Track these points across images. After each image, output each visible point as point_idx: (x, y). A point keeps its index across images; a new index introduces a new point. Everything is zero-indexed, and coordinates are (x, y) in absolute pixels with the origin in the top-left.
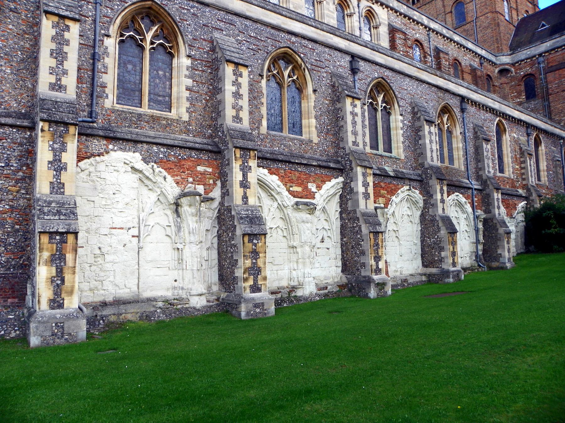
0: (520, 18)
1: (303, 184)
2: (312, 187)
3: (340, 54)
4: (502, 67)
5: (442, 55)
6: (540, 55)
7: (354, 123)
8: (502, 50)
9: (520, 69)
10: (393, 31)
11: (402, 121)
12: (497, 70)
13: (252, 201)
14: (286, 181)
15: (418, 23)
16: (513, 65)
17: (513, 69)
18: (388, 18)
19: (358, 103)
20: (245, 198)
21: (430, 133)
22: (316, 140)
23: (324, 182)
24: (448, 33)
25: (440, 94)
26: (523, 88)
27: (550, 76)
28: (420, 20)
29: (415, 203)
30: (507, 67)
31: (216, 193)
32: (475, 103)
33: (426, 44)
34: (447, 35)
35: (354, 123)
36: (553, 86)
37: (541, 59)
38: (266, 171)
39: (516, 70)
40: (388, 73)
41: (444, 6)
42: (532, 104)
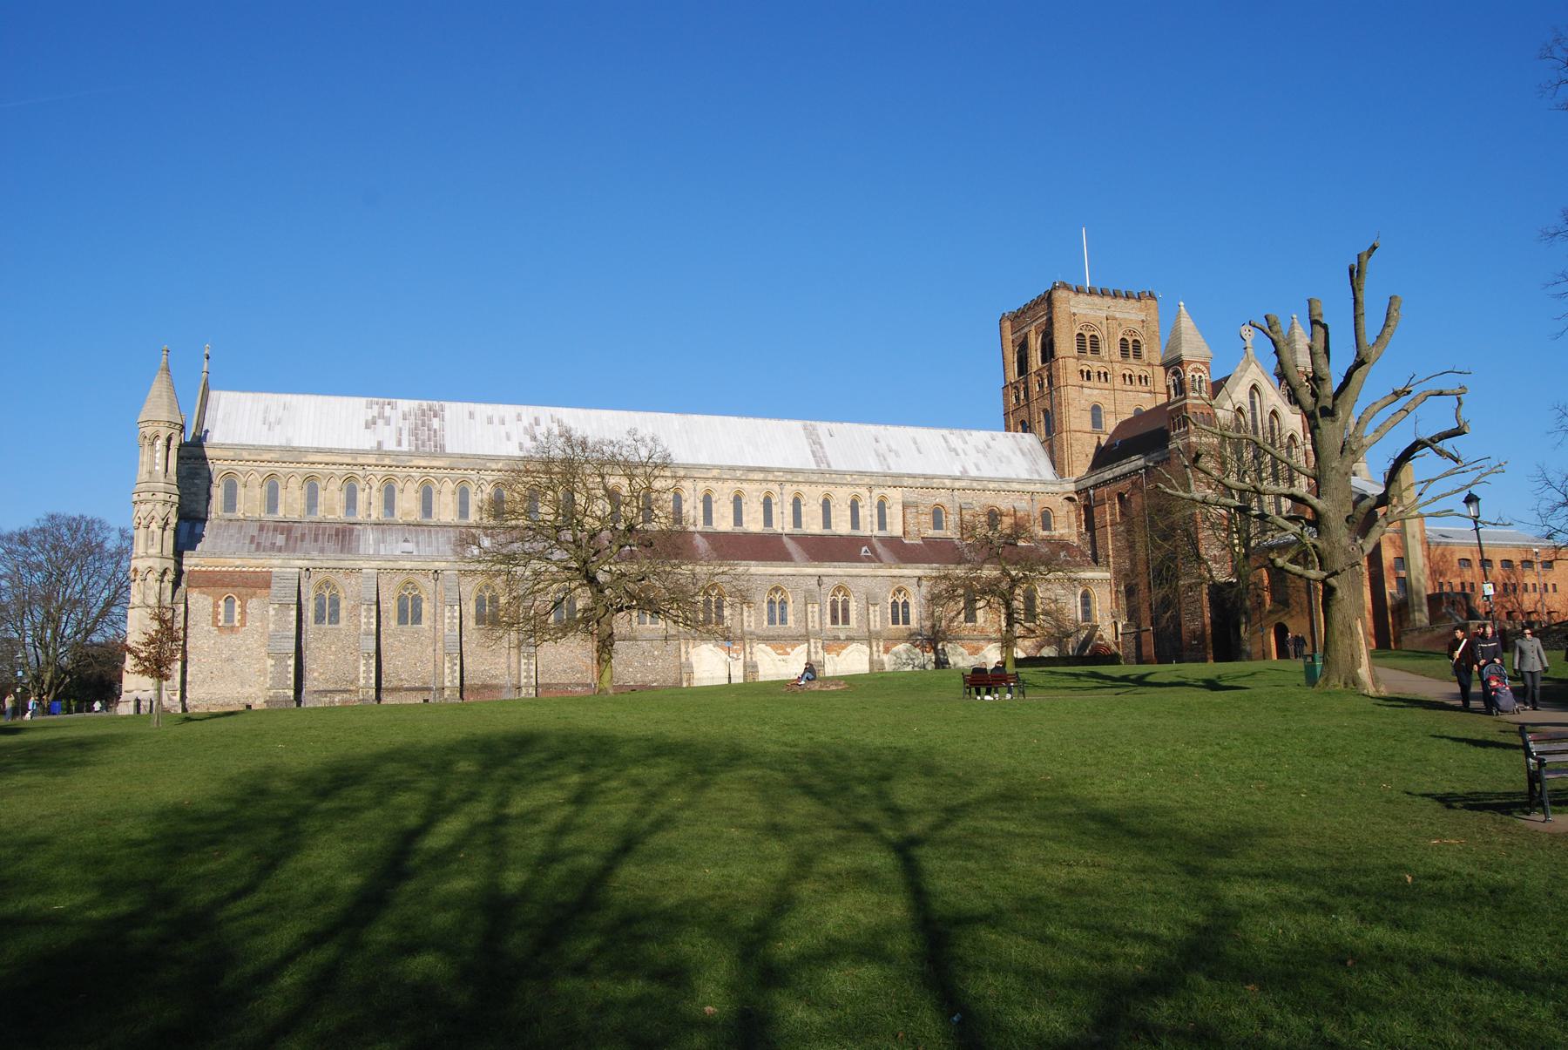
0: (1118, 422)
1: (782, 648)
2: (789, 650)
3: (810, 578)
5: (964, 512)
7: (813, 617)
10: (905, 506)
11: (857, 606)
12: (1061, 499)
13: (754, 659)
14: (775, 648)
15: (938, 489)
16: (1077, 492)
17: (1076, 498)
18: (903, 497)
19: (816, 606)
20: (751, 658)
21: (874, 611)
22: (793, 626)
23: (795, 647)
24: (979, 485)
25: (894, 580)
28: (941, 486)
29: (864, 652)
31: (742, 656)
33: (947, 506)
34: (979, 487)
35: (813, 617)
38: (764, 645)
40: (846, 578)
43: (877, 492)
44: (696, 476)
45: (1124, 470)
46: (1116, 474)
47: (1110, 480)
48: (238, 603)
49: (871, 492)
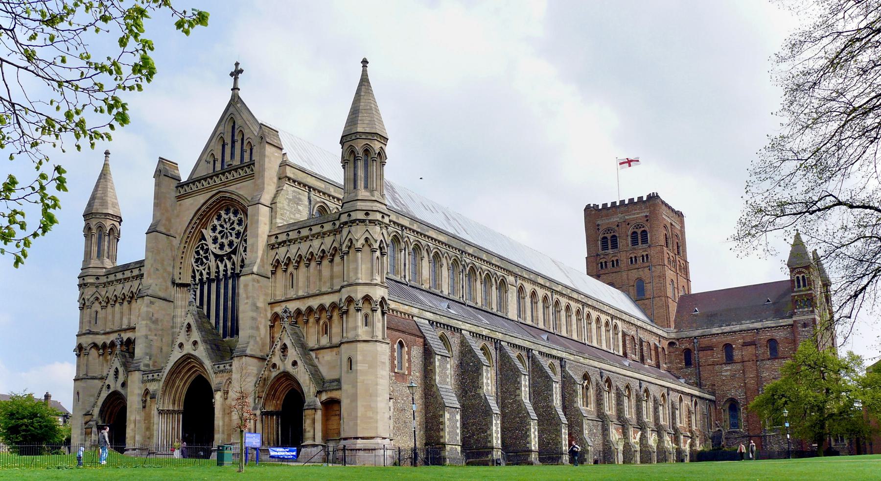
4: (671, 341)
6: (695, 338)
8: (670, 326)
9: (683, 344)
12: (668, 342)
16: (678, 340)
17: (677, 343)
26: (683, 357)
27: (701, 354)
30: (674, 341)
32: (673, 390)
33: (636, 337)
36: (702, 361)
37: (695, 341)
39: (680, 344)
41: (628, 279)
42: (689, 370)
43: (614, 321)
44: (553, 288)
45: (734, 329)
46: (724, 331)
47: (718, 334)
48: (406, 349)
49: (612, 320)
